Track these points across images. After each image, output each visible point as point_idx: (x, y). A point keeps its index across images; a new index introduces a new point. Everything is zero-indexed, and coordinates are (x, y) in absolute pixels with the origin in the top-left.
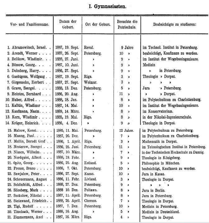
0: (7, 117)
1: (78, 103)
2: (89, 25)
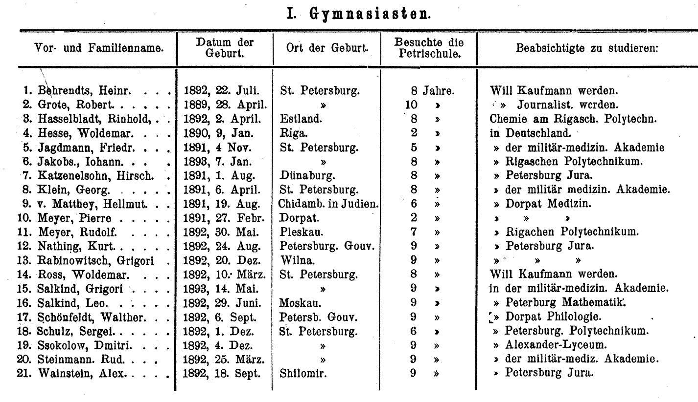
0: (22, 260)
2: (298, 49)
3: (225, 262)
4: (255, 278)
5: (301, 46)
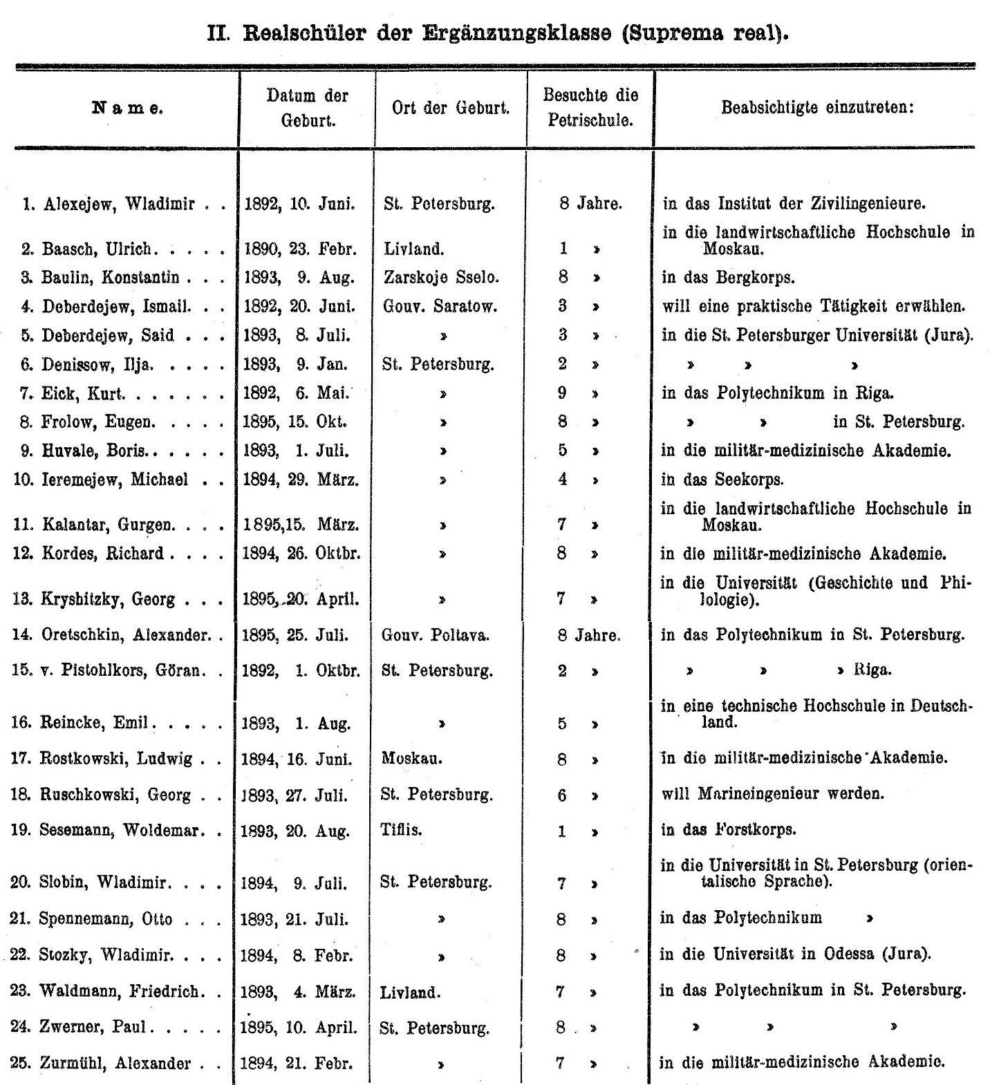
1: (353, 438)
2: (409, 110)
3: (299, 834)
4: (341, 997)
5: (413, 105)
